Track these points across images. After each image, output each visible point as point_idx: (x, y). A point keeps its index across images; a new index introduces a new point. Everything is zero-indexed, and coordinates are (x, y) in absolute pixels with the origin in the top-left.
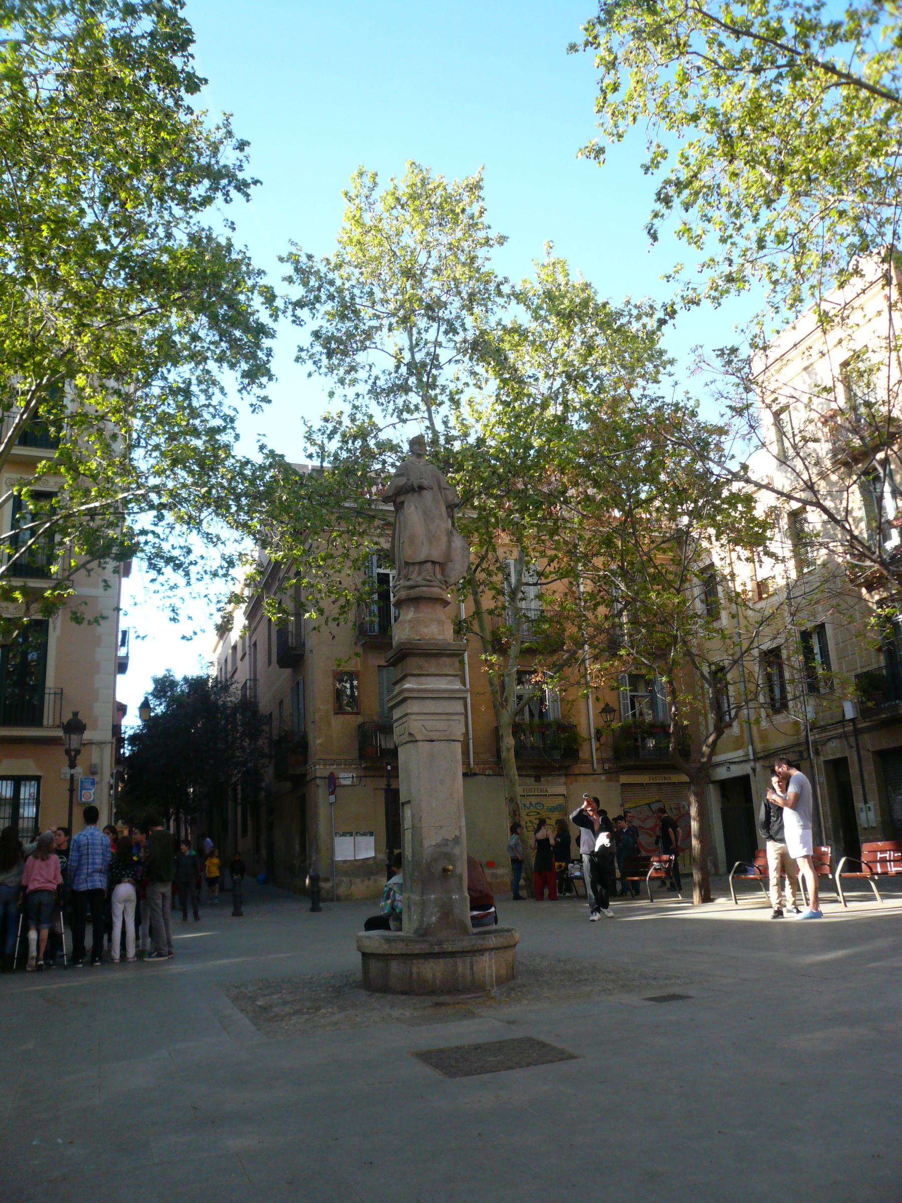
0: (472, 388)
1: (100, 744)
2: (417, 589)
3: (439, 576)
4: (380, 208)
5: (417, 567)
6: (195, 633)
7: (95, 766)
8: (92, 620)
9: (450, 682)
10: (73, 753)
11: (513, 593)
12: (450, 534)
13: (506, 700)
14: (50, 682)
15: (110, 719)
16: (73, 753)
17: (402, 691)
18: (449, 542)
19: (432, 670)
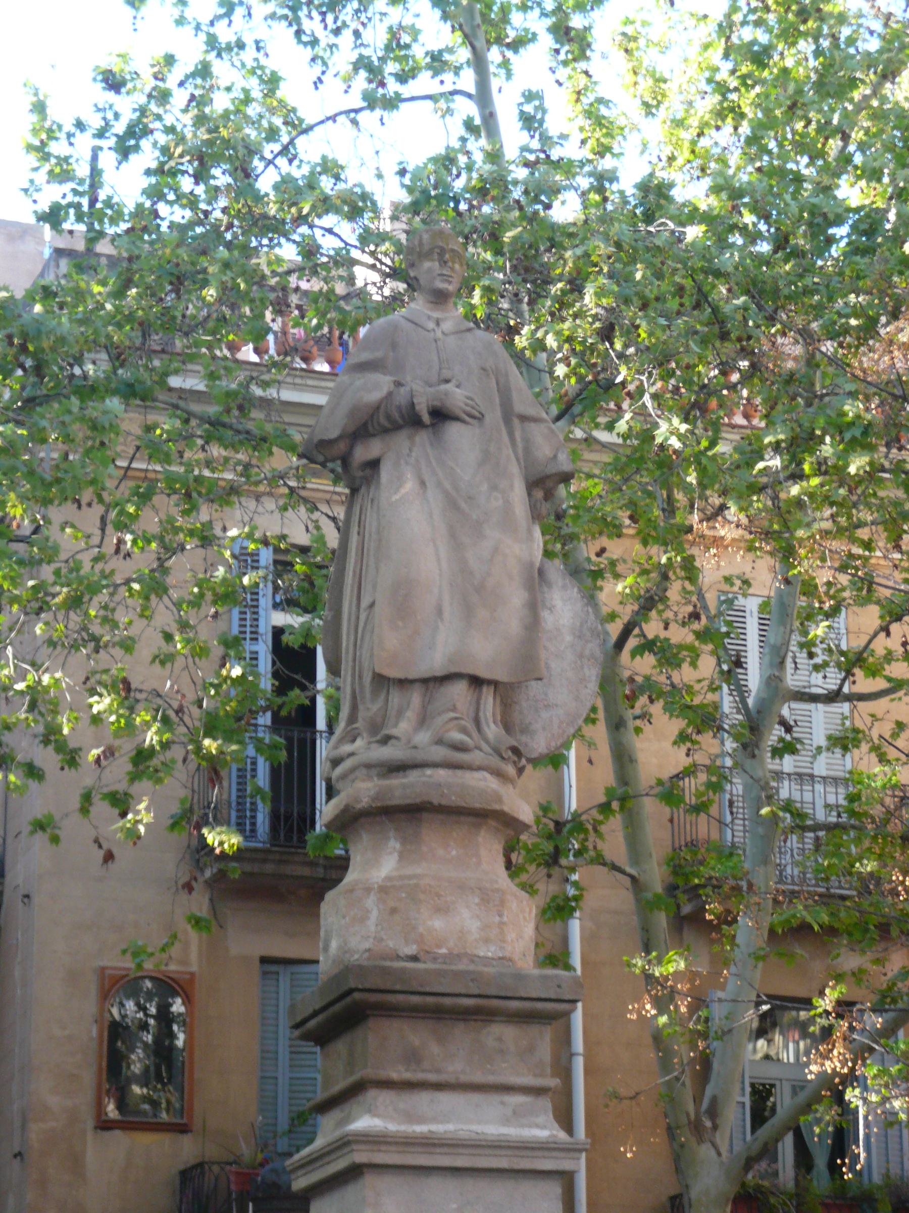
2: (413, 776)
3: (493, 730)
5: (416, 697)
9: (517, 1116)
12: (536, 580)
13: (713, 1112)
17: (345, 1143)
18: (534, 607)
19: (457, 1068)
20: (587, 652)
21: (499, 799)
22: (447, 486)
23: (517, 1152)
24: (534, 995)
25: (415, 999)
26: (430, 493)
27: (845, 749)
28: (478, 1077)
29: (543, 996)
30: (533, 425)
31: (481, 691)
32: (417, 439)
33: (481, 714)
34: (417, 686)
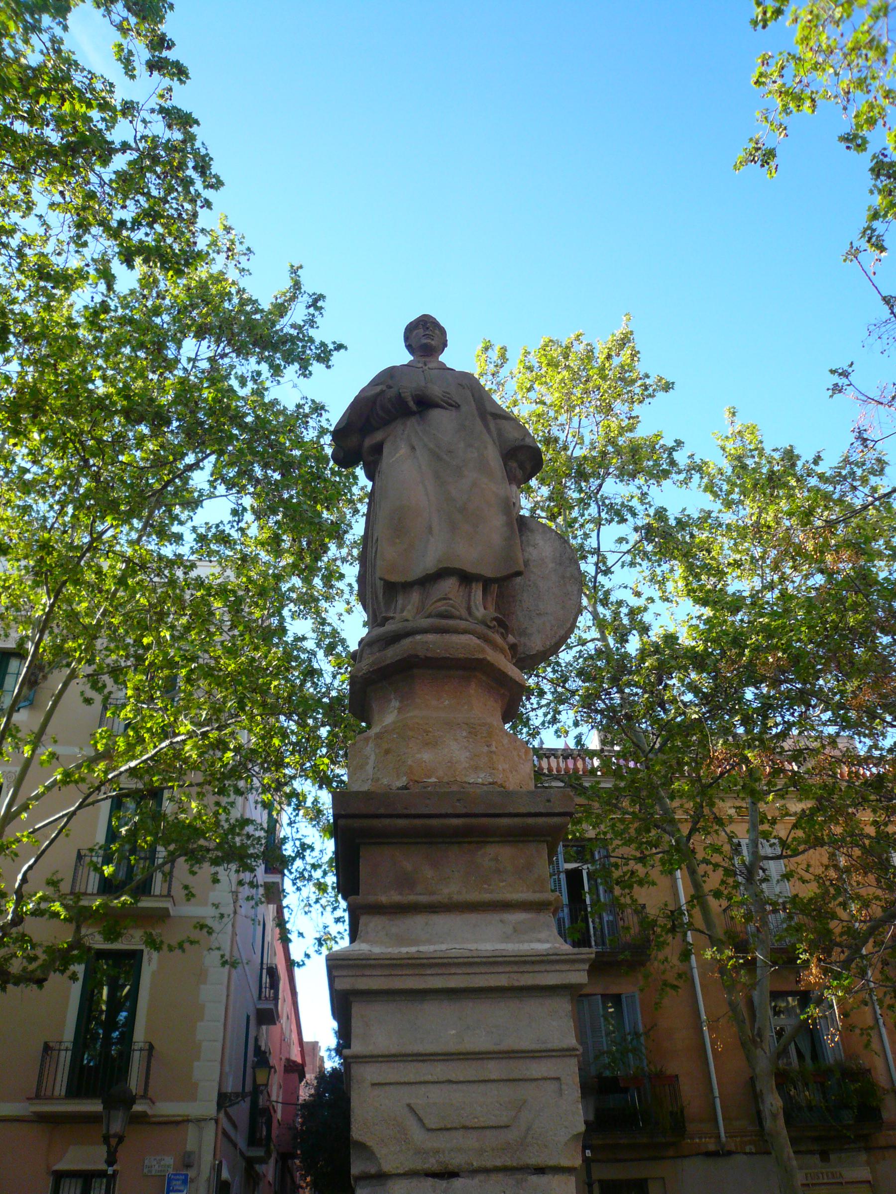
0: (658, 602)
1: (199, 1121)
2: (407, 642)
4: (512, 386)
5: (415, 596)
6: (307, 956)
7: (189, 1154)
8: (174, 943)
9: (518, 931)
10: (113, 1142)
11: (749, 873)
13: (760, 1035)
14: (140, 1035)
15: (216, 1085)
16: (113, 1142)
19: (453, 889)
20: (568, 575)
21: (483, 651)
22: (432, 446)
23: (515, 968)
24: (523, 810)
25: (401, 822)
26: (418, 452)
27: (788, 880)
28: (474, 896)
29: (532, 811)
31: (471, 588)
32: (409, 423)
33: (472, 604)
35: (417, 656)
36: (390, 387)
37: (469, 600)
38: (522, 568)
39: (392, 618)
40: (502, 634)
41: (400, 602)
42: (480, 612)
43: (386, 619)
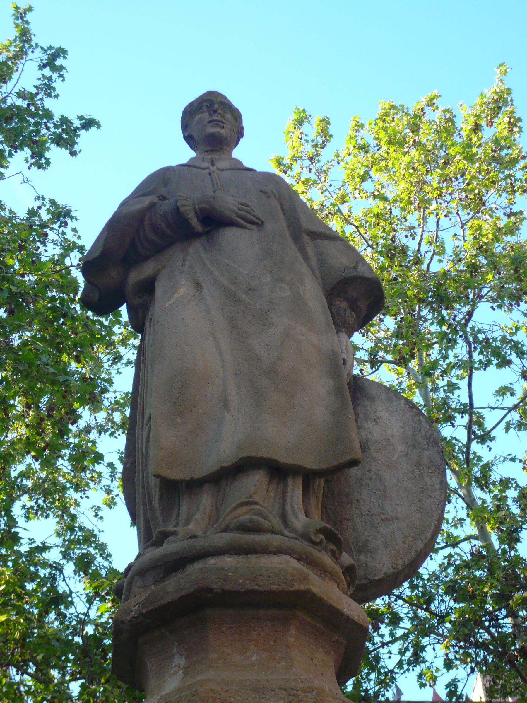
4: (338, 175)
5: (206, 500)
20: (425, 460)
21: (305, 579)
22: (224, 281)
30: (326, 242)
32: (191, 249)
33: (288, 508)
34: (207, 485)
35: (211, 590)
36: (163, 198)
37: (284, 504)
38: (358, 454)
39: (174, 533)
40: (333, 552)
41: (184, 508)
42: (299, 521)
43: (165, 535)
